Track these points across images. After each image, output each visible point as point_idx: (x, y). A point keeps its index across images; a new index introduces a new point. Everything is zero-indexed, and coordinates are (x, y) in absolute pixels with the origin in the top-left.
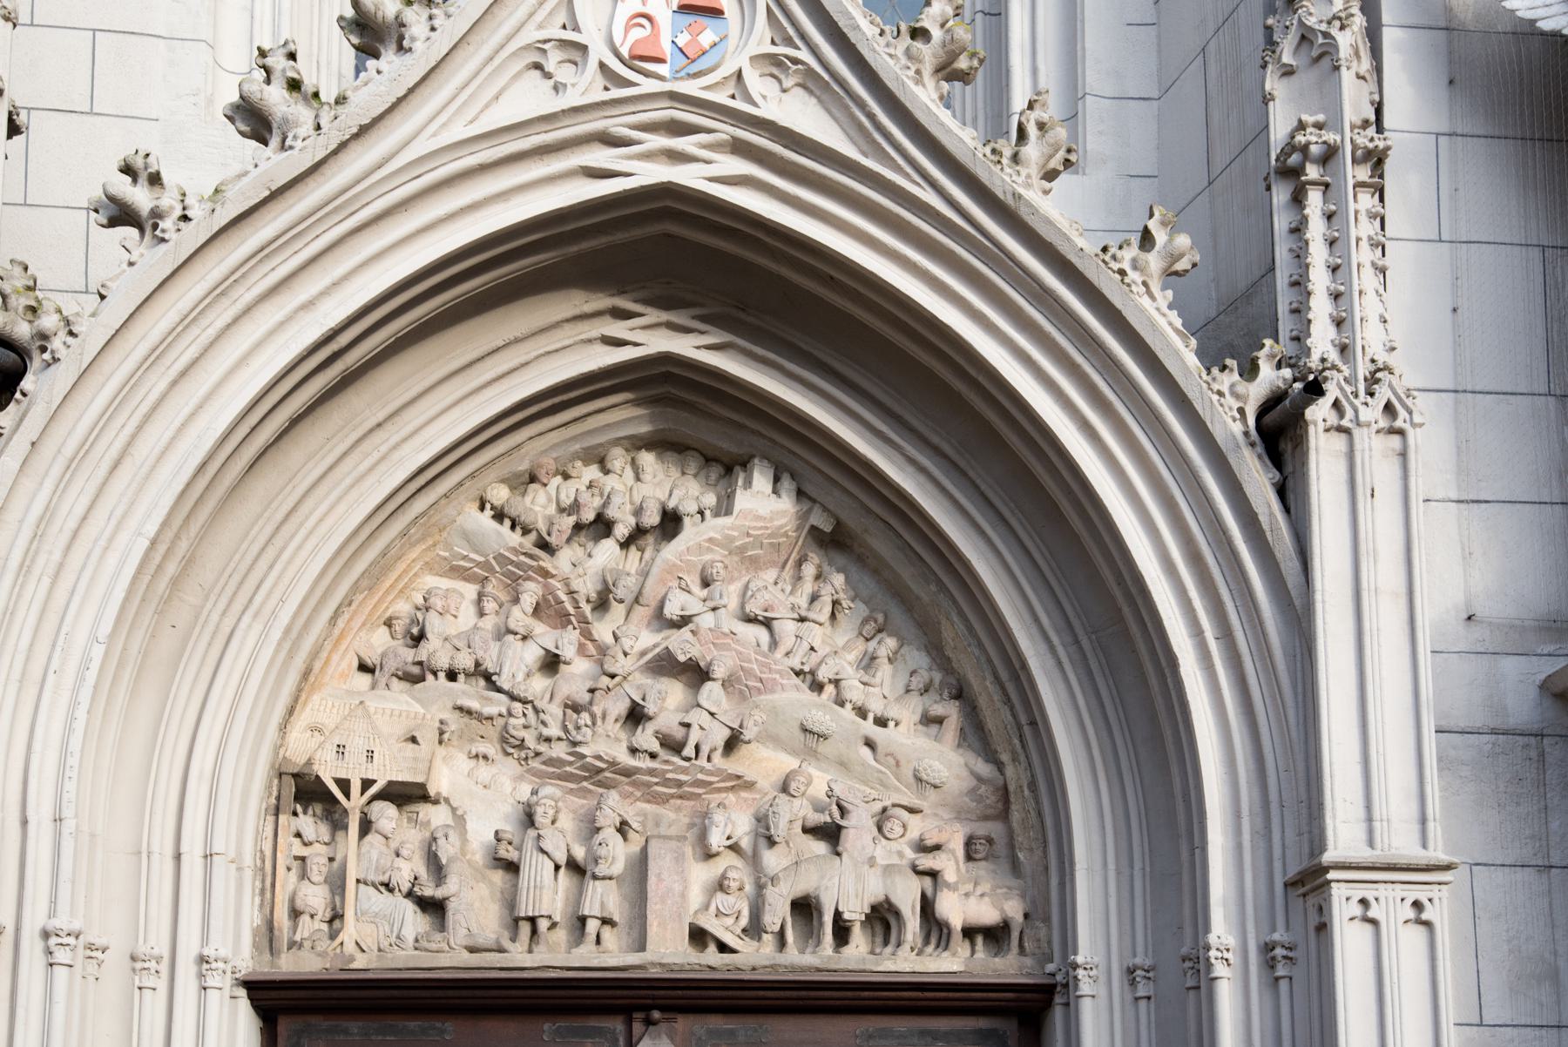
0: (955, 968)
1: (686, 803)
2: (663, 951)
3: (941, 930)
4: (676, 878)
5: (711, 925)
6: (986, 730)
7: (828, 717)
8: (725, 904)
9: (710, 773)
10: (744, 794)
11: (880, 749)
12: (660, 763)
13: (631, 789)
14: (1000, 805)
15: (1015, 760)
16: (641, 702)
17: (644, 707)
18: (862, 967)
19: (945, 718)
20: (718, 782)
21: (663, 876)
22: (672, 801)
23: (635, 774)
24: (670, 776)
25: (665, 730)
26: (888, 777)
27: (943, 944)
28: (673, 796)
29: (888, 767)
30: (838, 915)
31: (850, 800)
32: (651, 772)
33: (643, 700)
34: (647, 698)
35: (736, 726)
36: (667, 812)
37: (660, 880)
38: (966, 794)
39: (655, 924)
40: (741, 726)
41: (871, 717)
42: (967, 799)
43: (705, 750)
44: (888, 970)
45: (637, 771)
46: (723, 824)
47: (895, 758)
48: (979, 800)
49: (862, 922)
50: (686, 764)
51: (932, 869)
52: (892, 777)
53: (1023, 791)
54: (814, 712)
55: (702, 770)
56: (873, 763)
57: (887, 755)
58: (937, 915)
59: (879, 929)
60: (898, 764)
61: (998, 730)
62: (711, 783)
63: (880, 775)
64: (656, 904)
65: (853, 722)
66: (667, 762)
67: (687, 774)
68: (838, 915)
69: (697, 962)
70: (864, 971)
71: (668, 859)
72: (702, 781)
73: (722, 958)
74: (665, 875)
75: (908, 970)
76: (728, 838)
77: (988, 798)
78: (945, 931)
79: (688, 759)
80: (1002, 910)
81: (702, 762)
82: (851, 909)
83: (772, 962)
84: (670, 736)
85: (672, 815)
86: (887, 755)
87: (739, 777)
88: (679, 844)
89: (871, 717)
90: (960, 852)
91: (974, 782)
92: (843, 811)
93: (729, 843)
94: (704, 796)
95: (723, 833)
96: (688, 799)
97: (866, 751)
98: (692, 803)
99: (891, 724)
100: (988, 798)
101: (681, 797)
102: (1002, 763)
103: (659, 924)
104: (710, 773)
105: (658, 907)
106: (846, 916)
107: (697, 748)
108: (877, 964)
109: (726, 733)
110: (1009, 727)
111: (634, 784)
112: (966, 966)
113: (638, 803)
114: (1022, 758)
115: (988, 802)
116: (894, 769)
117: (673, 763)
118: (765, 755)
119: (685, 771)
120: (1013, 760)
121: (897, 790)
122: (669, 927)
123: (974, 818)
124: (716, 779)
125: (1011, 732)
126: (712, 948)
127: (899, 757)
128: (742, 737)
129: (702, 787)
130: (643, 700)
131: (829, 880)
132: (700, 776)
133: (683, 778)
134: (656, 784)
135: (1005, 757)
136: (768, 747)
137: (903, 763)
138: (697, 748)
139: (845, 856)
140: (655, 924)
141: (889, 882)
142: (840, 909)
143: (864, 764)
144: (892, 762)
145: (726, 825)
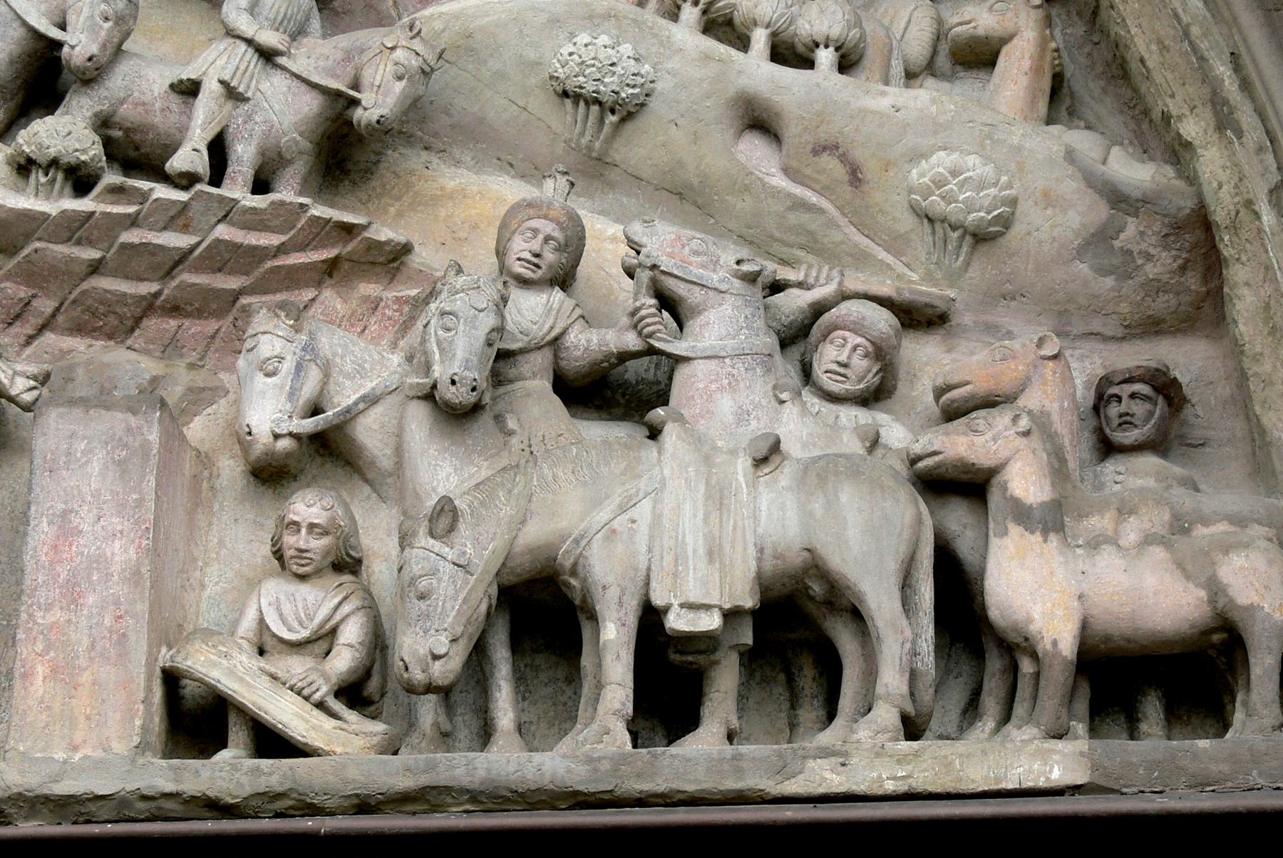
0: (1057, 775)
1: (194, 328)
2: (60, 755)
3: (1014, 668)
4: (116, 523)
5: (231, 672)
6: (1134, 66)
7: (627, 49)
8: (287, 608)
9: (255, 221)
10: (369, 289)
11: (791, 132)
12: (97, 199)
13: (23, 292)
14: (1193, 281)
15: (1224, 122)
16: (55, 33)
17: (58, 45)
18: (731, 784)
19: (1005, 41)
20: (281, 250)
21: (76, 521)
22: (155, 325)
23: (28, 237)
24: (131, 236)
25: (126, 112)
26: (832, 224)
27: (1020, 709)
28: (149, 306)
29: (823, 191)
30: (651, 617)
31: (696, 272)
32: (74, 228)
33: (63, 27)
34: (71, 18)
35: (334, 84)
36: (133, 355)
37: (66, 528)
38: (1080, 253)
39: (41, 670)
40: (356, 86)
41: (760, 39)
42: (1083, 268)
43: (244, 155)
44: (821, 790)
45: (31, 224)
46: (288, 366)
47: (843, 159)
48: (1125, 266)
49: (751, 659)
50: (182, 196)
51: (968, 468)
52: (843, 221)
53: (1257, 216)
54: (583, 38)
55: (228, 212)
56: (780, 181)
57: (819, 150)
58: (994, 614)
59: (808, 679)
60: (855, 176)
61: (1163, 48)
62: (258, 254)
63: (805, 217)
64: (48, 608)
65: (707, 57)
66: (117, 192)
67: (185, 229)
68: (651, 617)
69: (170, 787)
70: (741, 799)
71: (96, 467)
72: (235, 247)
73: (257, 771)
74: (84, 520)
75: (890, 787)
76: (315, 410)
77: (1149, 257)
78: (1026, 666)
79: (187, 180)
80: (1215, 589)
81: (236, 190)
82: (695, 596)
83: (423, 780)
84: (143, 128)
85: (149, 367)
86: (819, 150)
87: (348, 230)
88: (133, 421)
89: (760, 39)
90: (1065, 425)
91: (1102, 212)
92: (667, 303)
93: (308, 425)
94: (244, 300)
95: (292, 395)
96: (199, 314)
97: (754, 150)
98: (212, 326)
99: (825, 57)
100: (1149, 257)
101: (174, 309)
102: (1188, 145)
103: (54, 670)
104: (255, 221)
105: (57, 615)
106: (677, 622)
107: (218, 149)
108: (782, 771)
109: (310, 104)
110: (1195, 31)
111: (36, 275)
112: (1095, 767)
113: (49, 338)
114: (1246, 117)
115: (1151, 270)
116: (846, 191)
117: (143, 196)
118: (451, 185)
119: (177, 218)
120: (1221, 127)
121: (862, 259)
122: (86, 678)
123: (1112, 328)
124: (274, 240)
125: (1203, 45)
126: (238, 735)
127: (859, 154)
128: (358, 115)
129: (231, 272)
130: (63, 27)
131: (623, 509)
132: (223, 232)
133: (176, 240)
134: (95, 268)
135: (1191, 129)
136: (458, 163)
137: (871, 169)
138: (218, 149)
139: (671, 434)
140: (41, 670)
141: (817, 506)
142: (658, 600)
143: (747, 184)
144: (832, 166)
145: (299, 368)
